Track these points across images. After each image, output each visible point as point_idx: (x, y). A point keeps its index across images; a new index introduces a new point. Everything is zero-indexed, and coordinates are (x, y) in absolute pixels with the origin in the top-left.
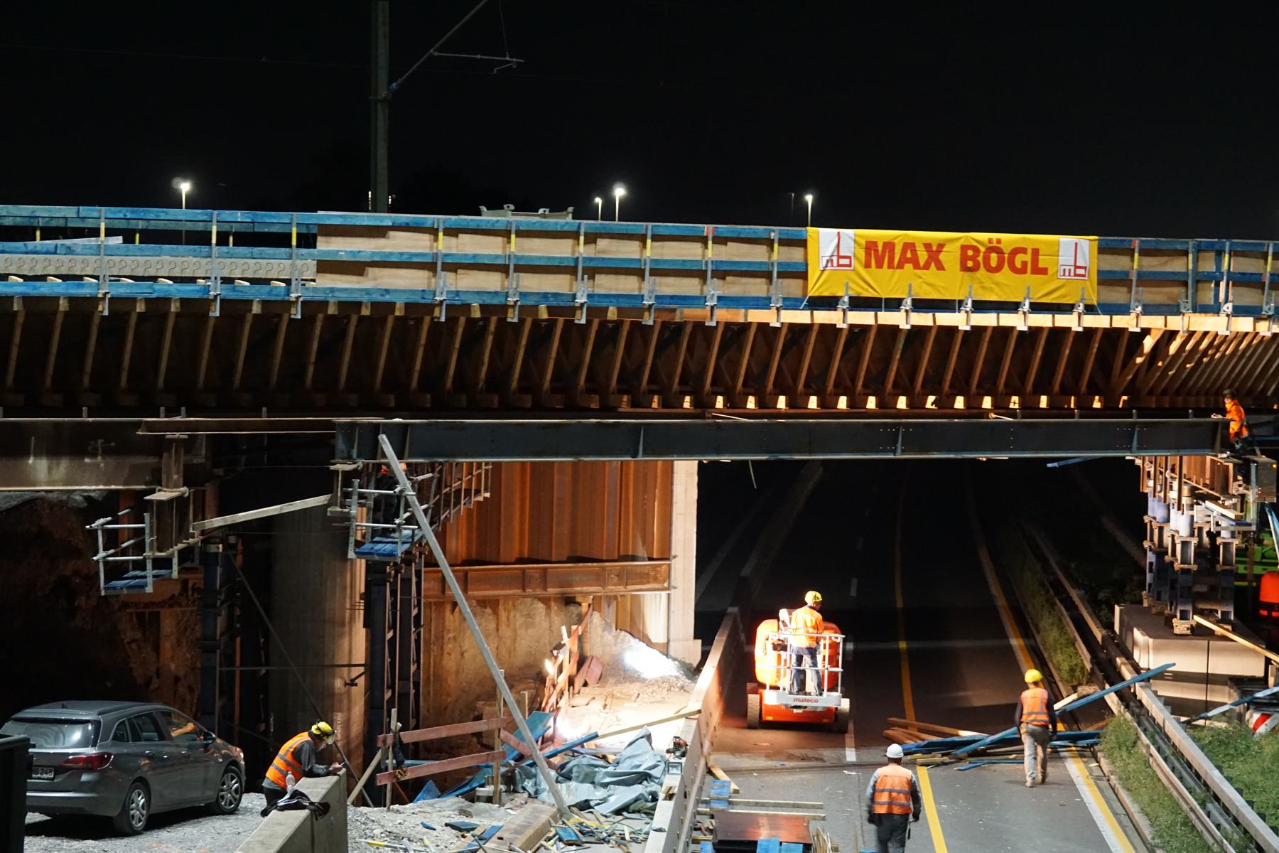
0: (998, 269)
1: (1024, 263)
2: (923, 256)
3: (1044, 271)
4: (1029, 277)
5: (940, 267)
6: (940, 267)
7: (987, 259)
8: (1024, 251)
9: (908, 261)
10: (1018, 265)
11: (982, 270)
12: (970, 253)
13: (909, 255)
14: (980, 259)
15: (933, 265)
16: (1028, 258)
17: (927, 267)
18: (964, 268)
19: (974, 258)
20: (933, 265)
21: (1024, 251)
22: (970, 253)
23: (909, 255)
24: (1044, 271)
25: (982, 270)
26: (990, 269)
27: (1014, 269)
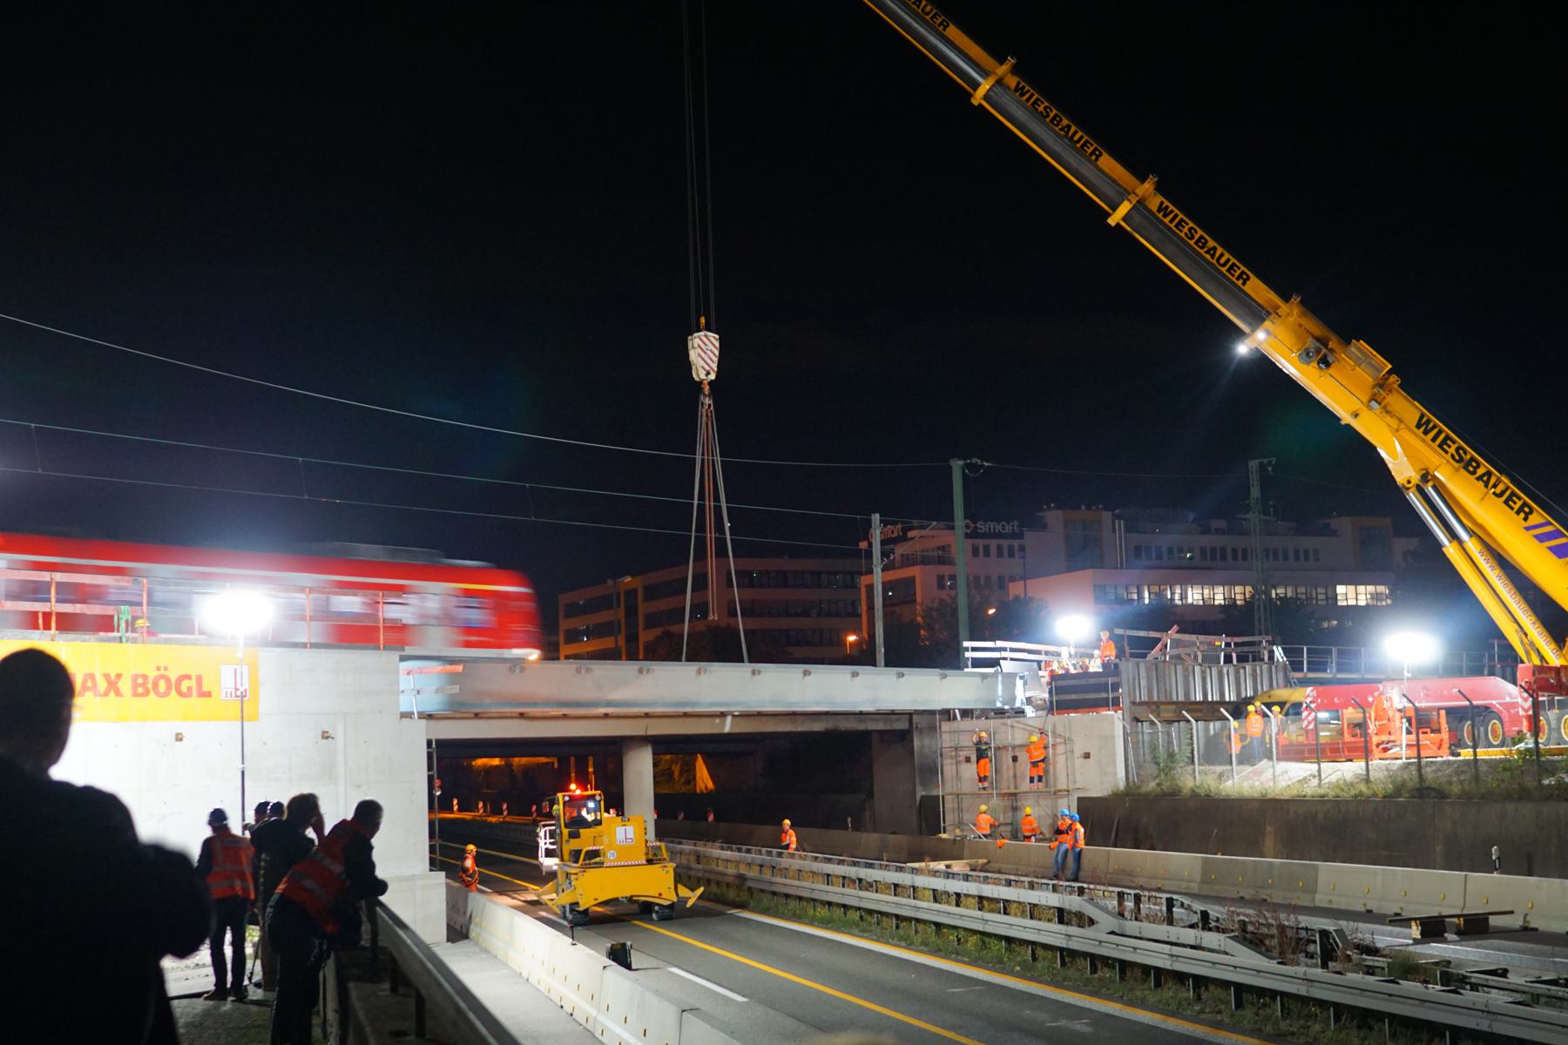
0: (166, 694)
1: (190, 689)
2: (102, 685)
3: (209, 695)
4: (194, 700)
5: (118, 693)
6: (118, 693)
7: (155, 685)
8: (188, 677)
9: (89, 689)
10: (184, 688)
11: (152, 694)
12: (140, 681)
13: (89, 684)
14: (150, 685)
15: (112, 694)
16: (193, 683)
17: (106, 694)
18: (135, 694)
19: (144, 685)
20: (112, 694)
21: (188, 677)
22: (140, 681)
23: (89, 684)
24: (209, 695)
25: (152, 694)
26: (158, 694)
27: (180, 693)
